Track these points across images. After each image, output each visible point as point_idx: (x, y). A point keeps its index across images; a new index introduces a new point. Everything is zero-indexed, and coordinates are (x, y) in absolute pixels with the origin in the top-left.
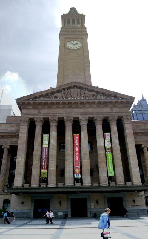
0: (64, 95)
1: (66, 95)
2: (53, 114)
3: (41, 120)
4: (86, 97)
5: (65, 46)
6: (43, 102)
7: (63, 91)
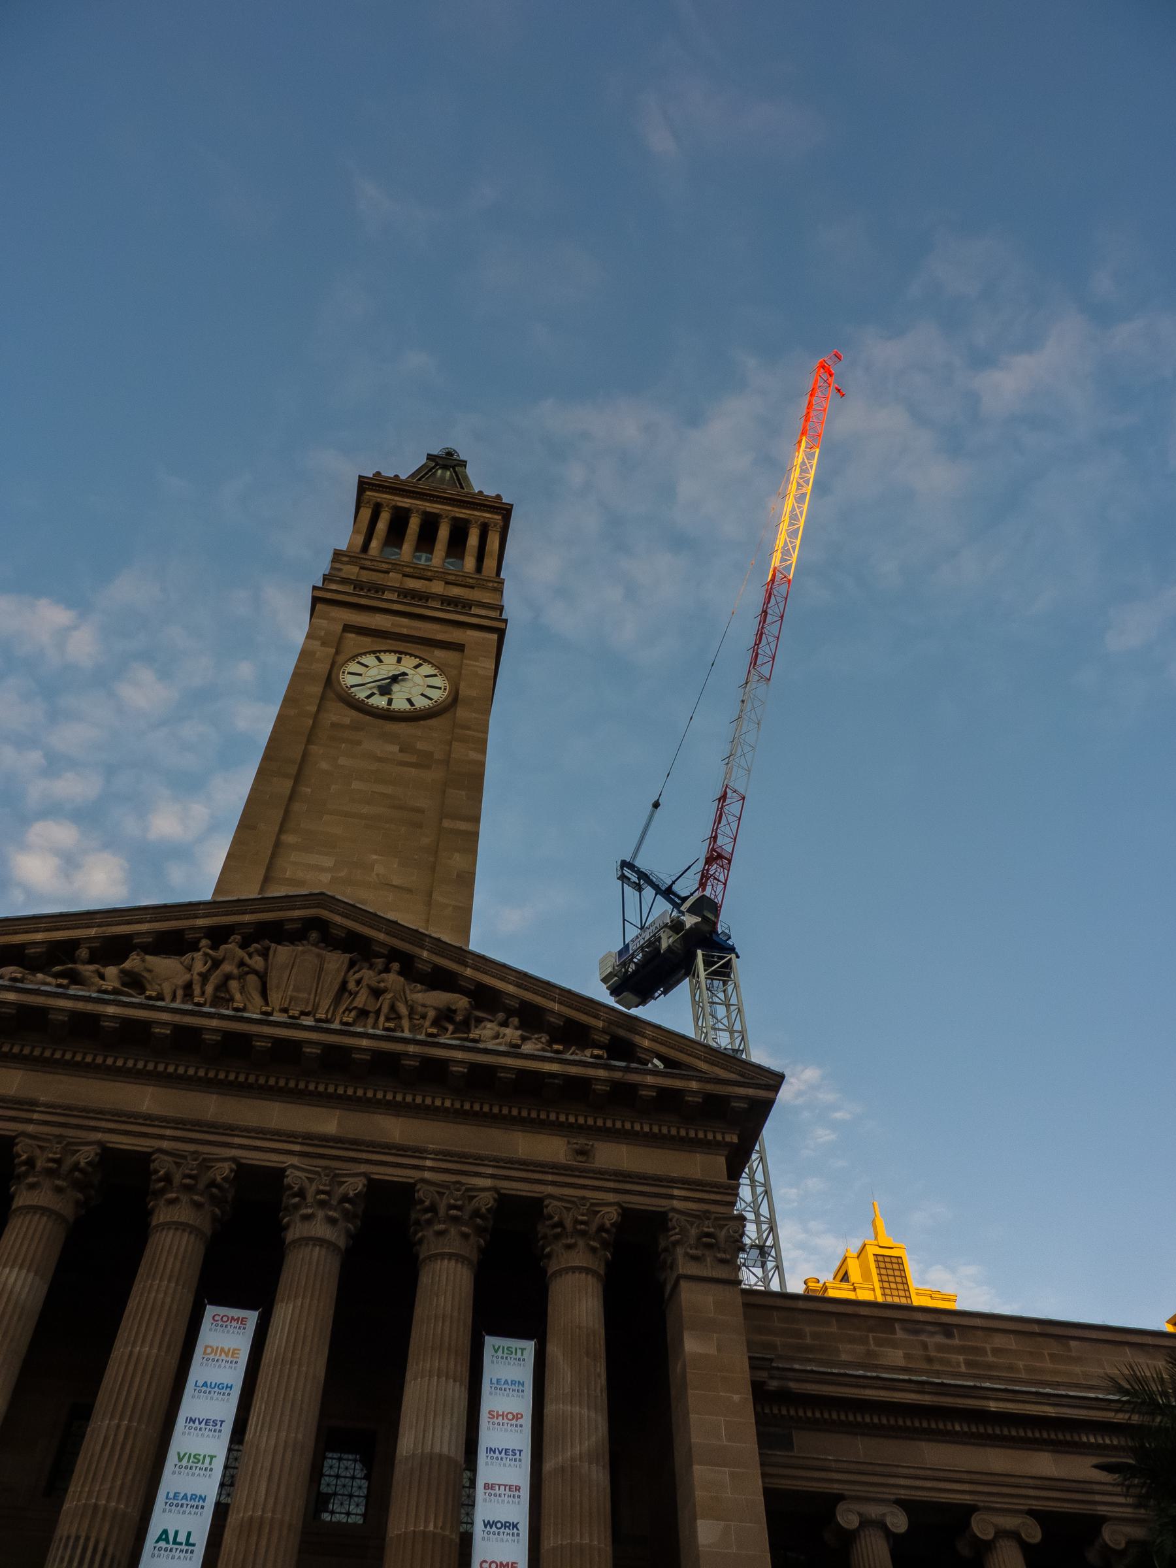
0: (205, 977)
4: (382, 1019)
5: (330, 681)
7: (204, 942)
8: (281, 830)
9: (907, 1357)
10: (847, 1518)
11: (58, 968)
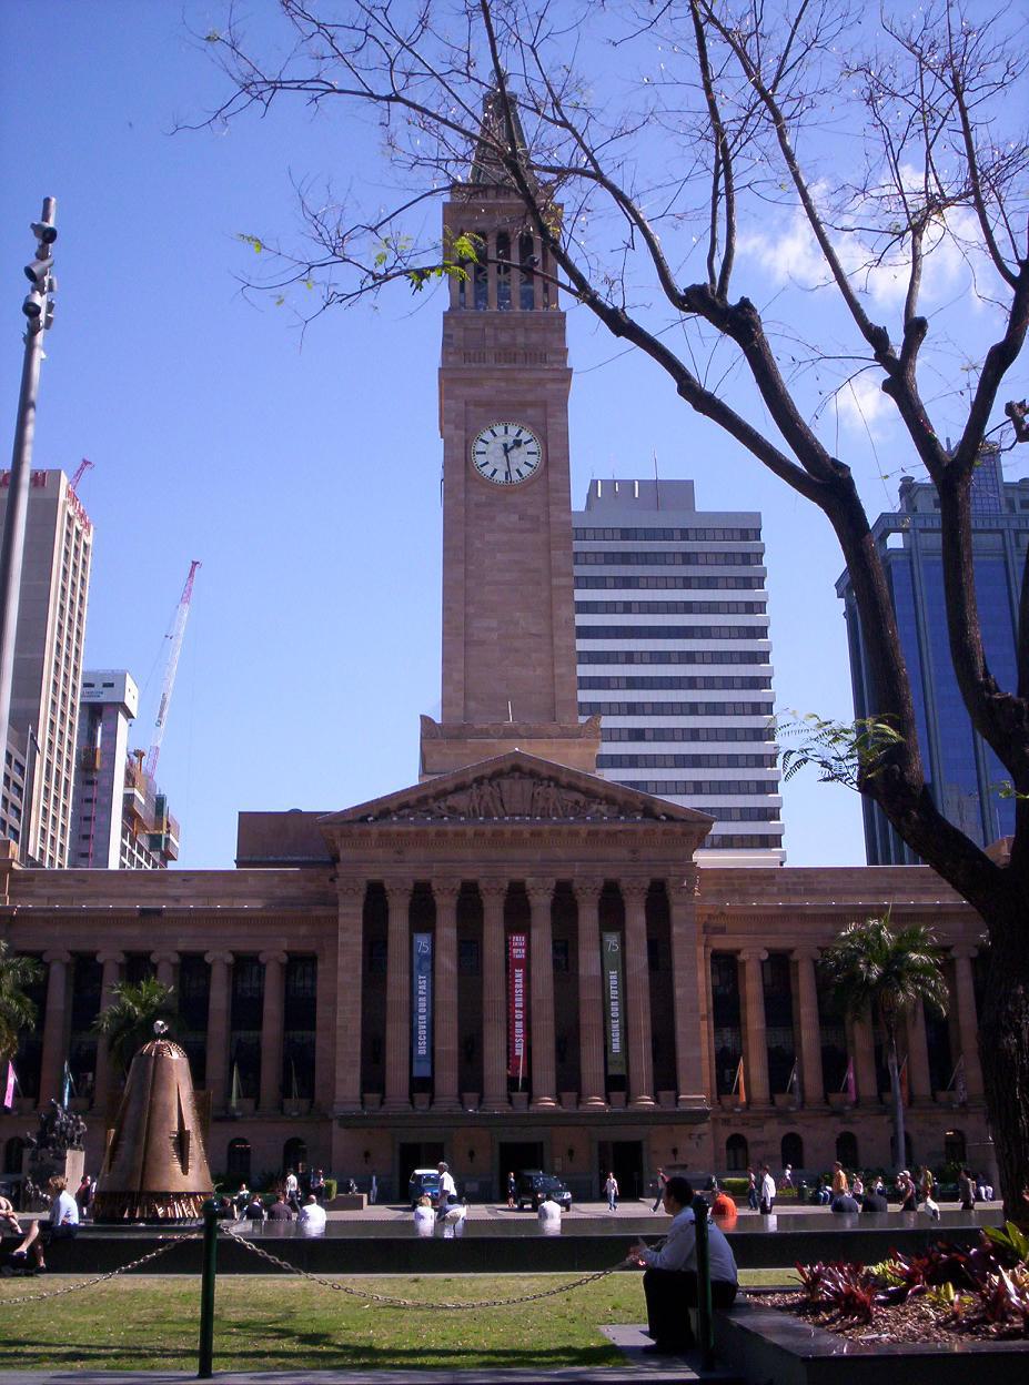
5: (467, 461)
7: (475, 785)
10: (742, 957)
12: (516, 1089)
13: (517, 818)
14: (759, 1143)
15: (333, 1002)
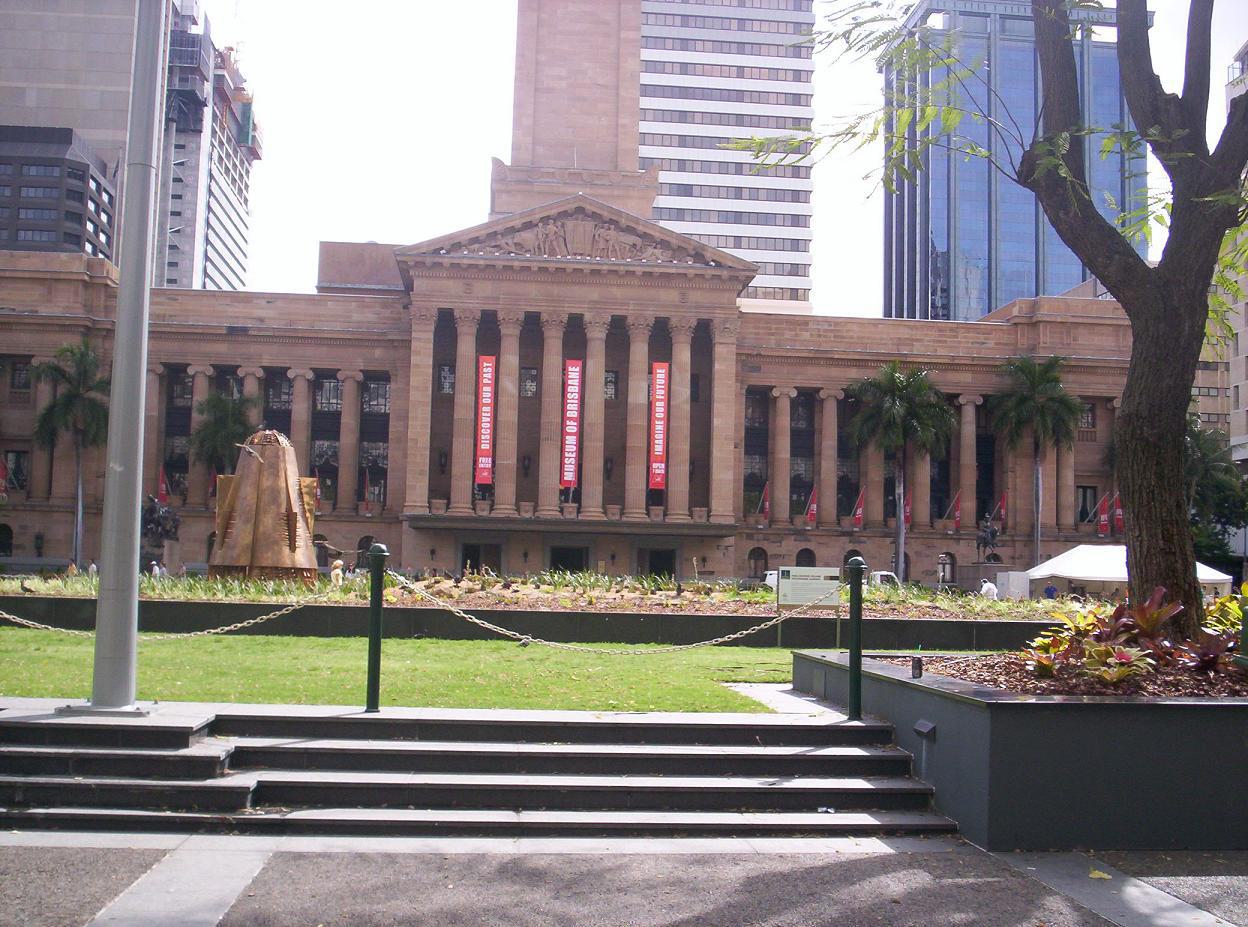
1: (551, 242)
2: (513, 300)
3: (474, 318)
6: (482, 262)
8: (538, 52)
9: (811, 335)
10: (775, 393)
11: (494, 244)
12: (566, 501)
13: (579, 258)
14: (777, 556)
15: (405, 418)
